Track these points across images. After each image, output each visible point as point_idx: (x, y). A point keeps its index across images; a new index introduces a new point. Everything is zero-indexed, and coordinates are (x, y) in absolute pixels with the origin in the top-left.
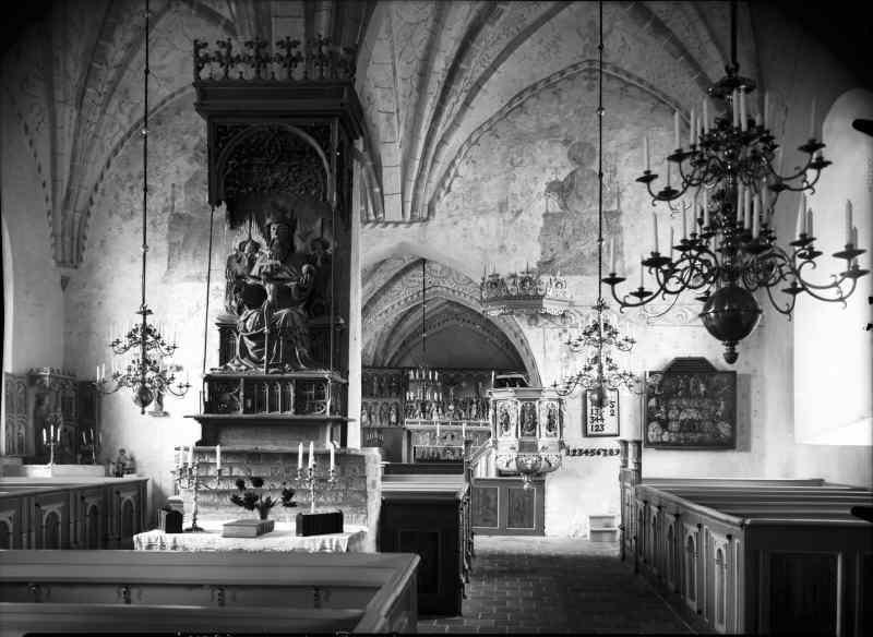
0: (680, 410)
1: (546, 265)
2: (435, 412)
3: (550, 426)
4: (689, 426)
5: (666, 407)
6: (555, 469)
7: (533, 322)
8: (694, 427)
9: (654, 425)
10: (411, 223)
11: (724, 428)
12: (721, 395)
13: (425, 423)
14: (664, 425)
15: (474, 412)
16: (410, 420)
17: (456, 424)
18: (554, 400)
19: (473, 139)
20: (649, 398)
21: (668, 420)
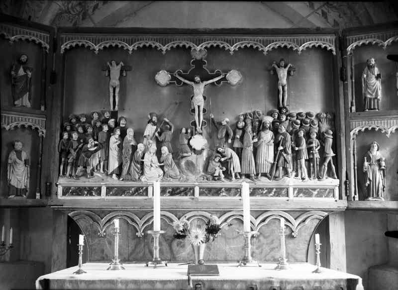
2: (150, 158)
13: (121, 191)
15: (267, 154)
16: (74, 183)
17: (217, 192)
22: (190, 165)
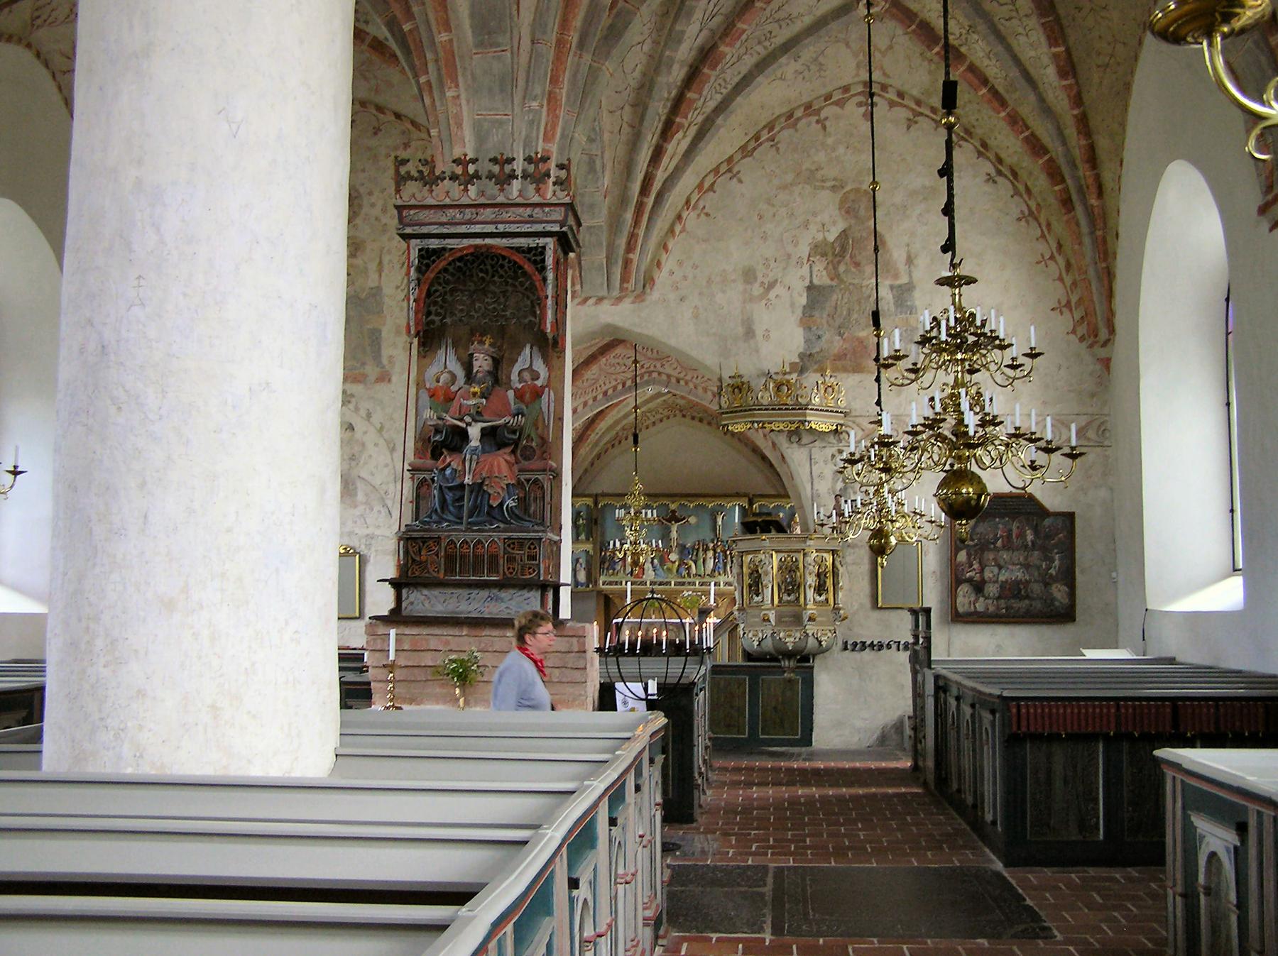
0: (1000, 568)
1: (807, 361)
2: (648, 566)
3: (820, 589)
4: (1012, 591)
5: (980, 563)
6: (827, 650)
7: (794, 438)
8: (1020, 590)
9: (964, 589)
10: (619, 300)
11: (1059, 592)
12: (1056, 546)
14: (979, 588)
15: (710, 564)
17: (683, 584)
18: (827, 551)
19: (706, 185)
20: (957, 550)
21: (983, 582)
22: (669, 570)
